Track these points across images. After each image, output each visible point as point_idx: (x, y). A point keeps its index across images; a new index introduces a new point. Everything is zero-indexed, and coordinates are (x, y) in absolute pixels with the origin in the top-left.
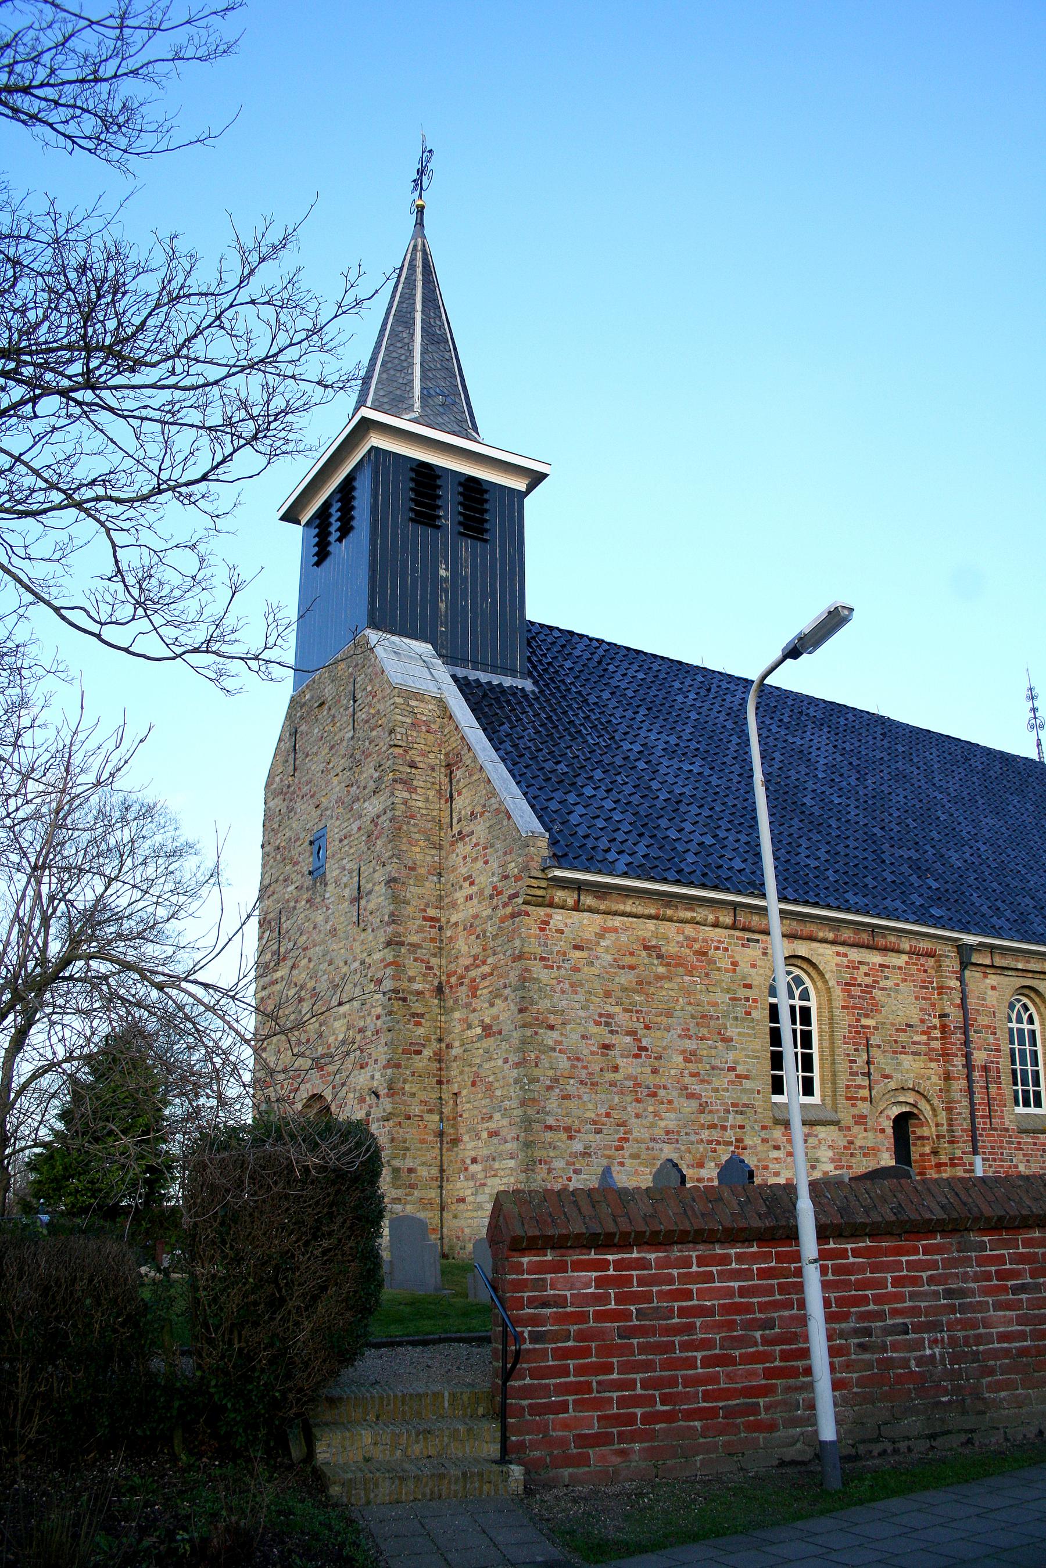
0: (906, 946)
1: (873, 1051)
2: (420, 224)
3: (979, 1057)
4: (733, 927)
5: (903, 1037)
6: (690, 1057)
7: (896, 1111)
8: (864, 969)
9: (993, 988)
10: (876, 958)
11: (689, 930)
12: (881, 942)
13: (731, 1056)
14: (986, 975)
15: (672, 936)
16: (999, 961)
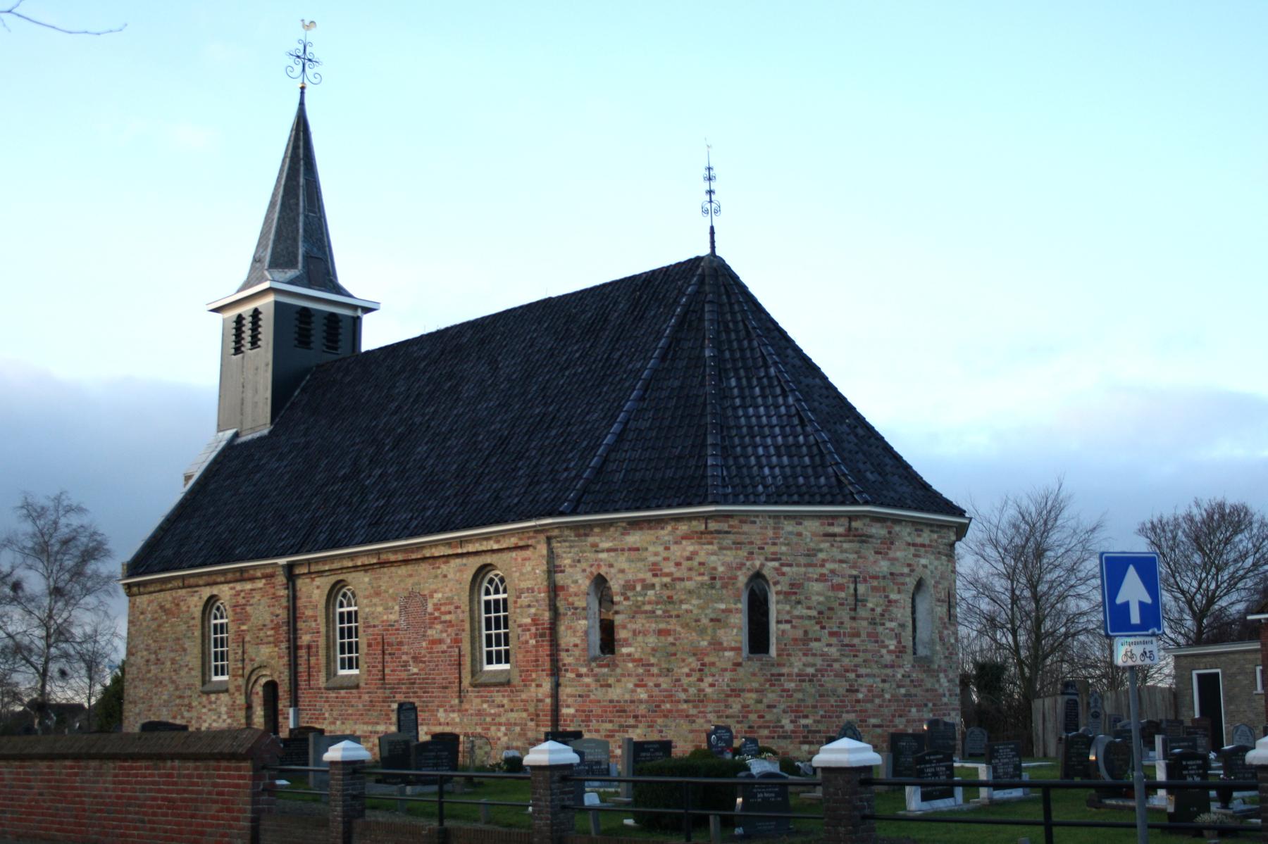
0: (259, 574)
1: (247, 646)
2: (302, 93)
3: (305, 639)
4: (184, 587)
5: (261, 634)
6: (173, 661)
7: (263, 681)
8: (242, 594)
9: (318, 587)
10: (248, 586)
11: (174, 593)
12: (246, 575)
13: (188, 658)
14: (313, 579)
15: (166, 598)
16: (314, 568)
